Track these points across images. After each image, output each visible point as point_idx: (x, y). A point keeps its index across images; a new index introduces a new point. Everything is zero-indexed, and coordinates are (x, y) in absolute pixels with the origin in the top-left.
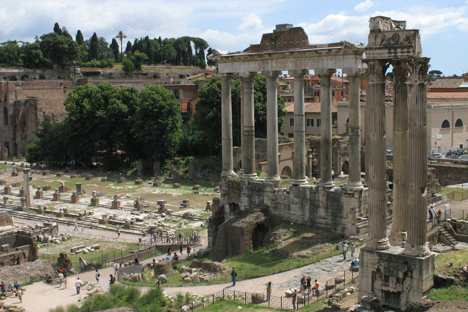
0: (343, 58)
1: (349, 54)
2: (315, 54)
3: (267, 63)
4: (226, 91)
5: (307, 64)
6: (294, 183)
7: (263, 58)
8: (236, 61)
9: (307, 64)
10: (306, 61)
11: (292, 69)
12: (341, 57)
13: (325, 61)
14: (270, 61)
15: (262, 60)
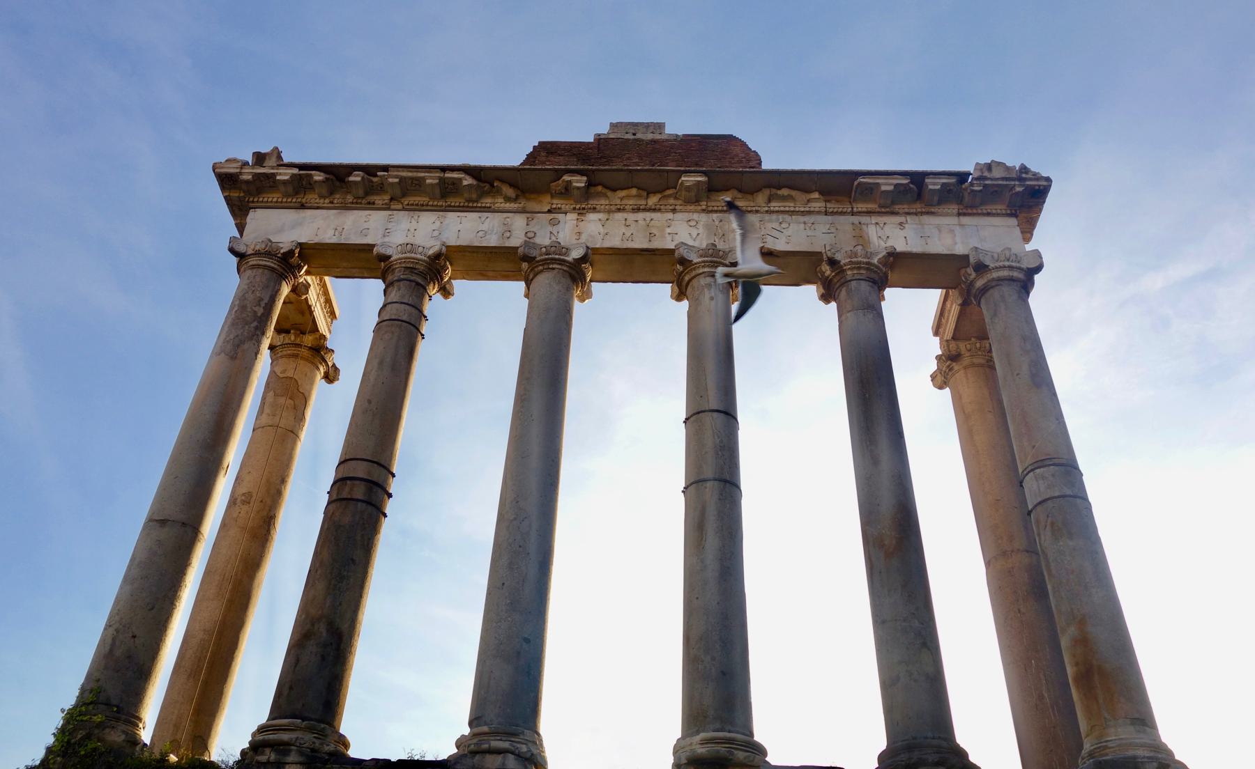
0: (962, 225)
1: (989, 214)
2: (818, 205)
3: (554, 223)
4: (260, 311)
5: (775, 233)
6: (722, 749)
7: (532, 205)
8: (371, 206)
9: (775, 233)
10: (769, 225)
11: (691, 243)
12: (953, 220)
13: (872, 232)
14: (572, 217)
15: (523, 211)
